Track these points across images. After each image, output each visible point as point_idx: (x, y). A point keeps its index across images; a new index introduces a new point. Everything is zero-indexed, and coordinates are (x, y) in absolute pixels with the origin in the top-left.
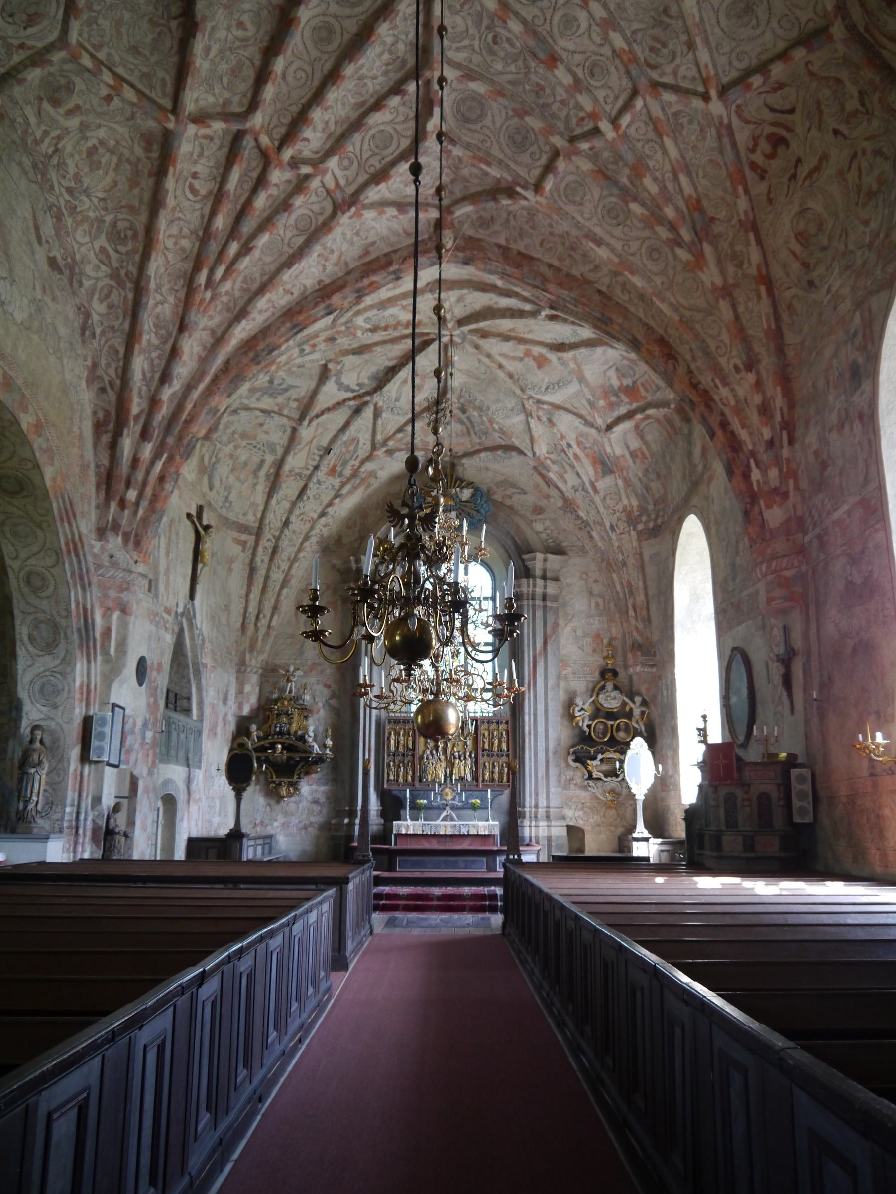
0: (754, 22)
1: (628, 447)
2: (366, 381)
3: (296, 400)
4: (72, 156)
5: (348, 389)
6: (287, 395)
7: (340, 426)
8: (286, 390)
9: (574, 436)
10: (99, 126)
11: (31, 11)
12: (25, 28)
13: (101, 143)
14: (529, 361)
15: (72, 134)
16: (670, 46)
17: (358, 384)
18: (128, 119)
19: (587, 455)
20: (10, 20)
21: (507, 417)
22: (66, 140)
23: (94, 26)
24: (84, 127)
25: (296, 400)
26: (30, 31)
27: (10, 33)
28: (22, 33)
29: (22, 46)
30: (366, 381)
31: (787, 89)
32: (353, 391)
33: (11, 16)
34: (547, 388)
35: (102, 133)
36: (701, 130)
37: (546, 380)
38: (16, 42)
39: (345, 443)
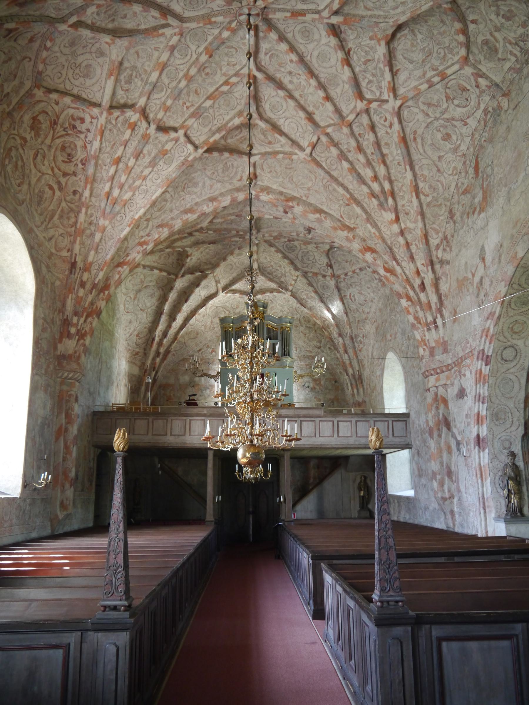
0: (67, 45)
4: (515, 32)
10: (490, 20)
11: (459, 91)
12: (468, 90)
13: (498, 15)
15: (505, 35)
16: (103, 15)
18: (474, 7)
20: (469, 99)
22: (509, 38)
23: (451, 46)
24: (497, 29)
26: (469, 88)
27: (475, 96)
28: (472, 90)
29: (477, 87)
31: (27, 42)
33: (467, 99)
35: (493, 17)
36: (60, 9)
38: (477, 90)
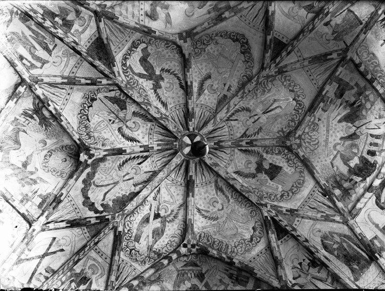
1: (377, 226)
2: (111, 204)
3: (40, 196)
5: (92, 207)
6: (35, 187)
7: (76, 250)
8: (35, 182)
9: (319, 240)
14: (263, 176)
17: (102, 205)
19: (338, 257)
21: (249, 251)
25: (40, 196)
30: (111, 204)
32: (96, 211)
34: (282, 196)
37: (280, 189)
39: (77, 275)
